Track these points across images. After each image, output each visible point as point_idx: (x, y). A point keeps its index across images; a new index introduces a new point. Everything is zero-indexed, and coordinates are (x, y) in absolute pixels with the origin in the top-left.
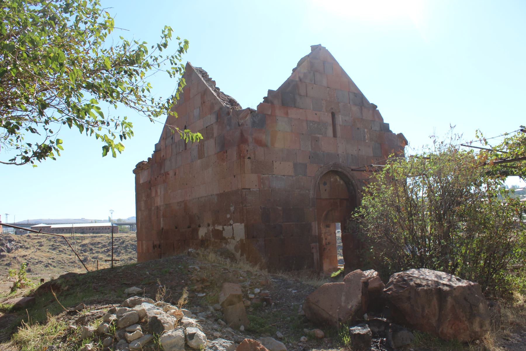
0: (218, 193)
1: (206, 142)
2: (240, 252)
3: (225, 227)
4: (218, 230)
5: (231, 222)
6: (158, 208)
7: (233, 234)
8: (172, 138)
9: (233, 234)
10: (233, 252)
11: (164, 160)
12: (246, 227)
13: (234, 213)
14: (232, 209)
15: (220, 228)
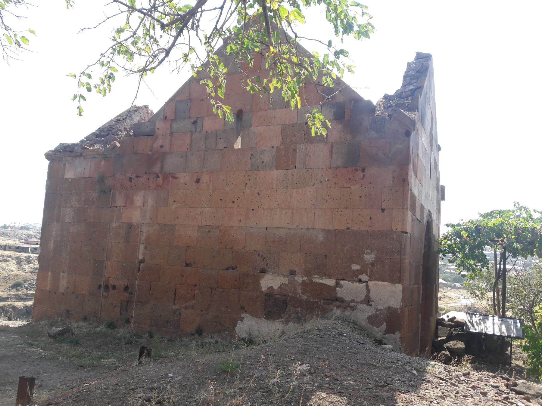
0: (331, 227)
1: (303, 146)
2: (384, 326)
3: (342, 282)
4: (322, 284)
5: (364, 277)
6: (130, 226)
7: (368, 296)
8: (195, 123)
9: (368, 296)
10: (364, 323)
11: (164, 154)
12: (404, 290)
13: (372, 264)
14: (369, 257)
15: (331, 282)
